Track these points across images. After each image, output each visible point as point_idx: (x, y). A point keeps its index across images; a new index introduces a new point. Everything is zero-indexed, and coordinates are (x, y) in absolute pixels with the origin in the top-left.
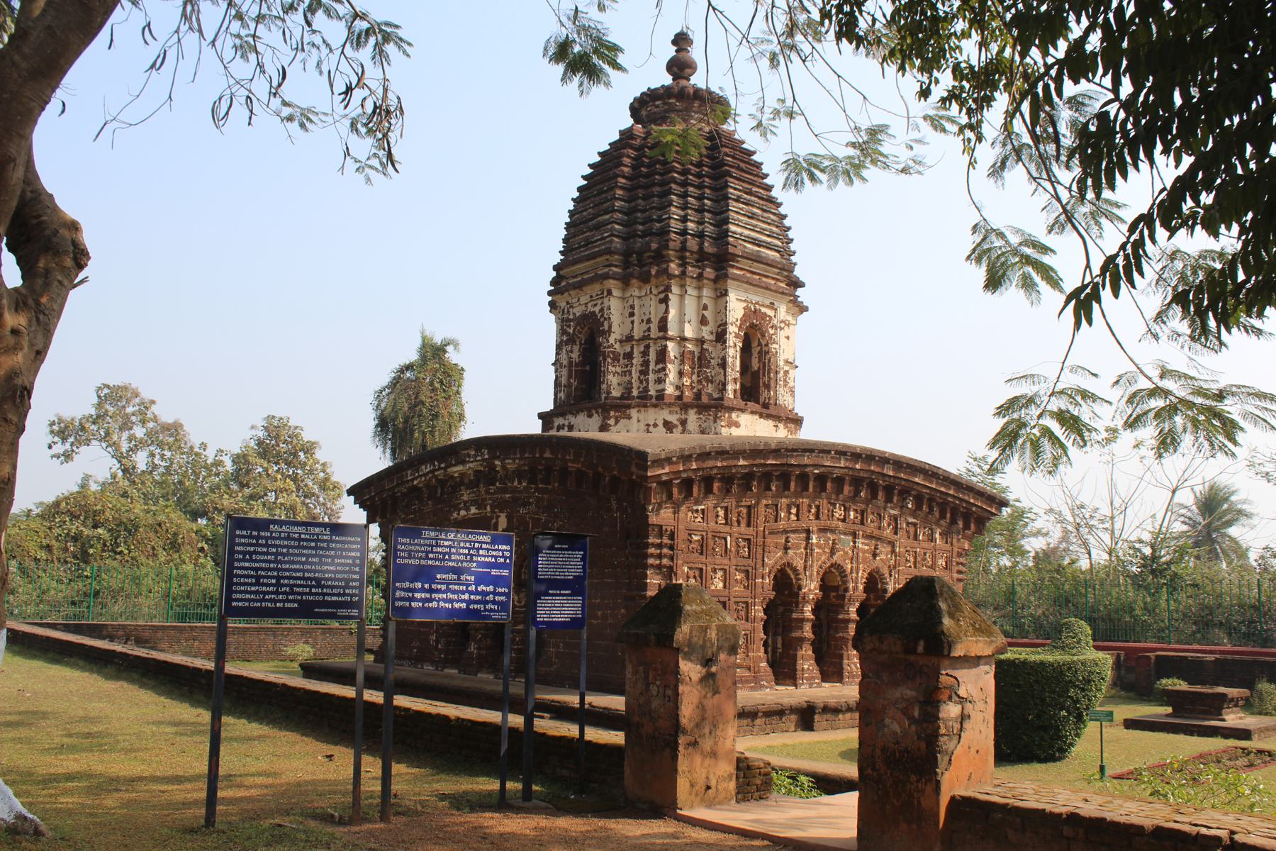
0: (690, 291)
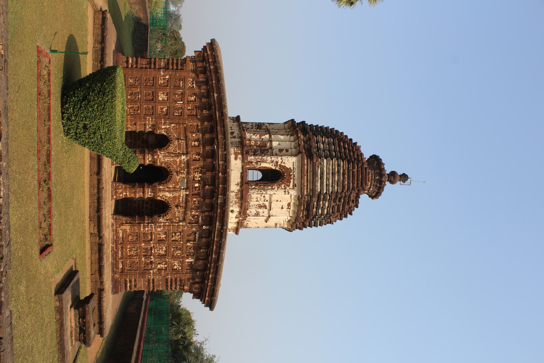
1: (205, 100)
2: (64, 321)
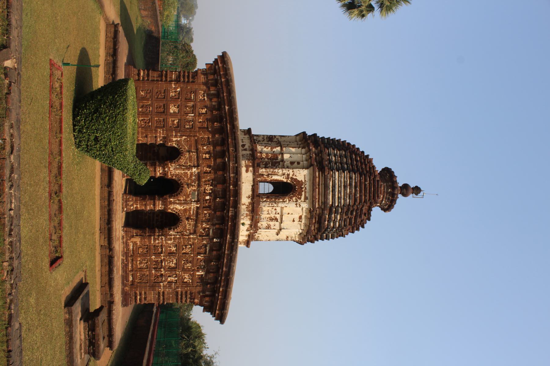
0: (304, 156)
1: (216, 113)
2: (74, 334)
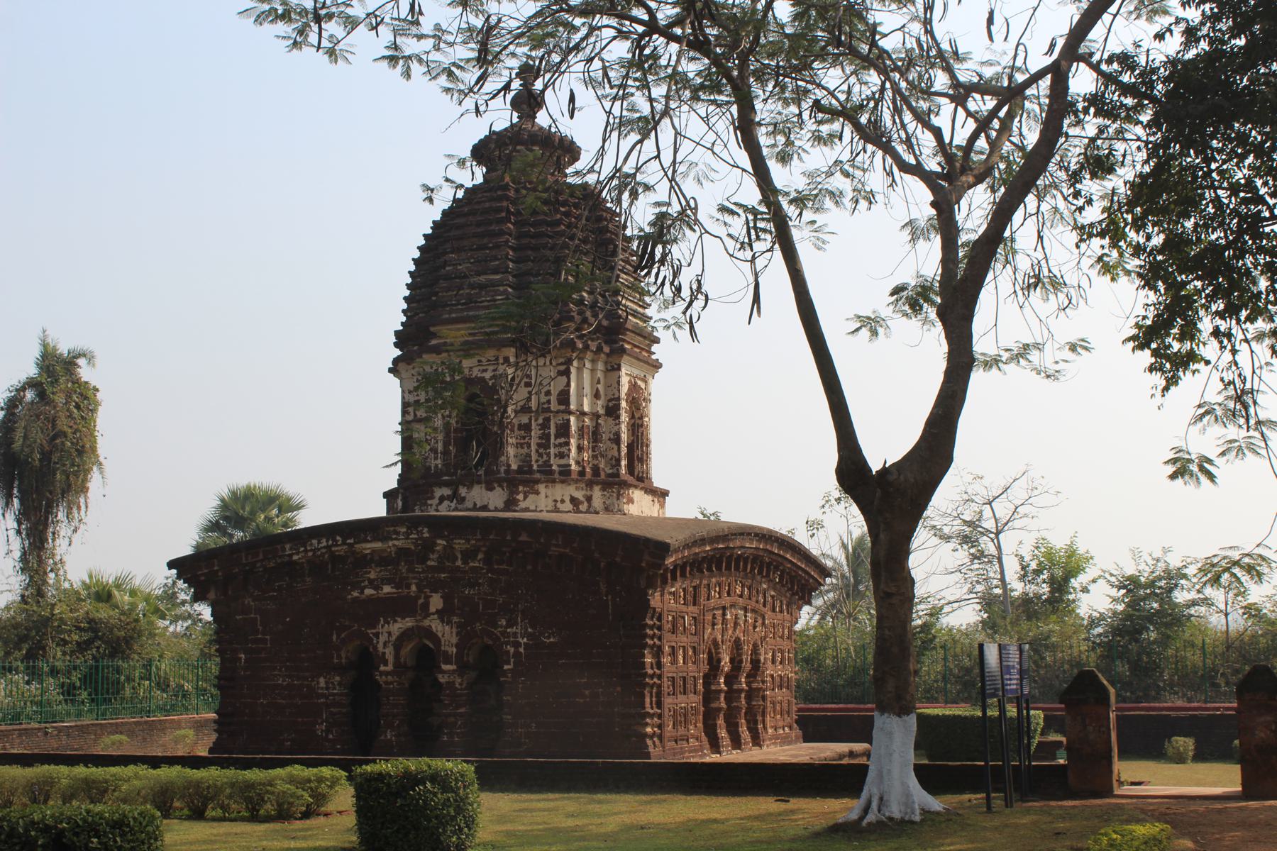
0: (588, 365)
